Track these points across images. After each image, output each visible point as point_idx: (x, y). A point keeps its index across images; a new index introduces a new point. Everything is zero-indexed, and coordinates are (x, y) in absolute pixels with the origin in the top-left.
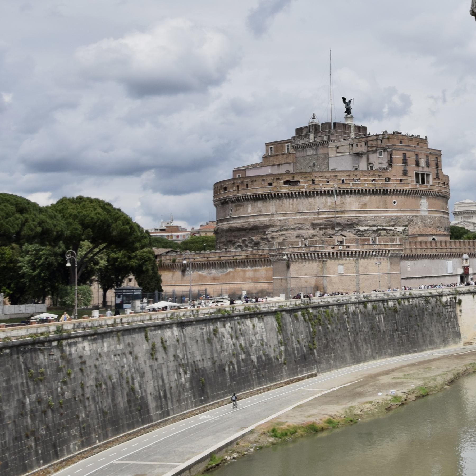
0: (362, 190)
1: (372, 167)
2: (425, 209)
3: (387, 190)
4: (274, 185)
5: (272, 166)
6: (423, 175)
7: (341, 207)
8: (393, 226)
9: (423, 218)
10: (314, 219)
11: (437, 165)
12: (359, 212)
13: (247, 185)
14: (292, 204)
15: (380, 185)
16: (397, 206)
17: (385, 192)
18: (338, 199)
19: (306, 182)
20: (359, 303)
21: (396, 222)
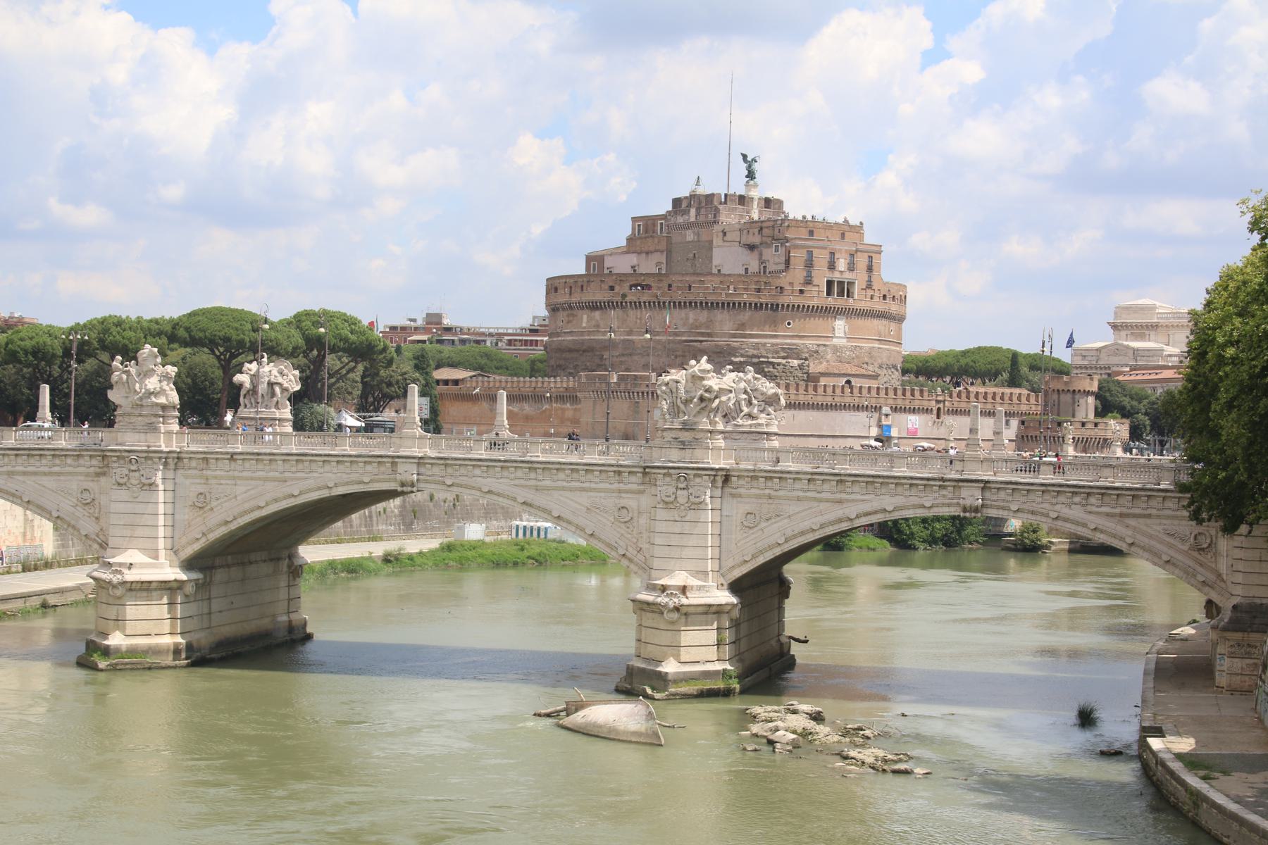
5: (639, 253)
6: (841, 283)
7: (708, 327)
8: (784, 358)
9: (836, 349)
10: (669, 342)
12: (734, 336)
18: (703, 316)
19: (659, 288)
21: (792, 353)
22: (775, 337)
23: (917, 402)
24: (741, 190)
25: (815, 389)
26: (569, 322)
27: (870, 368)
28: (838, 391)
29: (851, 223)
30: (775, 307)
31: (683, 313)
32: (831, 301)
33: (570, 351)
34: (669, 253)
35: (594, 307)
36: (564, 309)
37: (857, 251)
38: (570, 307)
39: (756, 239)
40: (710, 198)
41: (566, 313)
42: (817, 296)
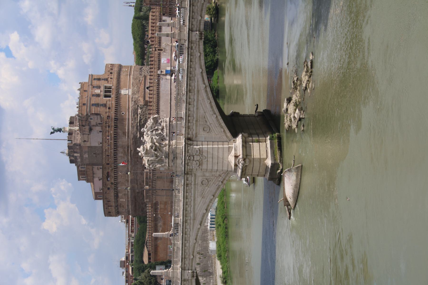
0: (115, 134)
1: (99, 124)
2: (128, 91)
3: (115, 118)
5: (93, 177)
6: (106, 92)
7: (125, 148)
8: (137, 116)
9: (133, 94)
10: (131, 164)
11: (99, 79)
12: (128, 136)
13: (108, 201)
14: (122, 176)
18: (120, 150)
19: (108, 168)
23: (156, 59)
24: (66, 134)
25: (150, 102)
26: (123, 207)
27: (141, 79)
28: (151, 92)
29: (80, 88)
30: (116, 119)
31: (119, 158)
33: (135, 206)
35: (117, 196)
36: (118, 209)
37: (92, 85)
38: (117, 206)
39: (87, 128)
40: (69, 147)
41: (119, 208)
42: (111, 101)
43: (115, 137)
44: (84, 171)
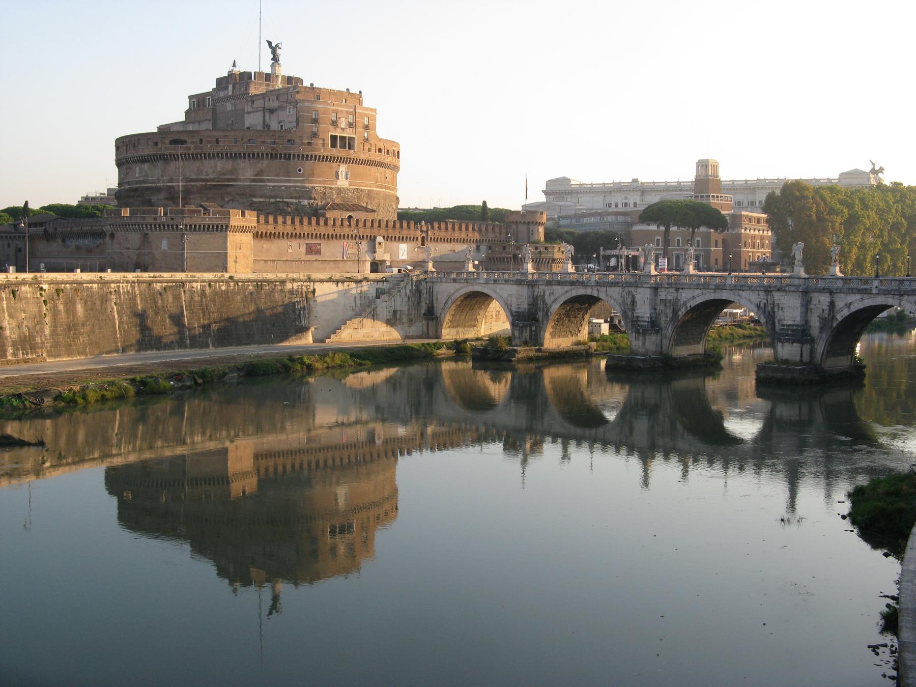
0: (258, 154)
3: (290, 155)
4: (160, 146)
7: (232, 174)
9: (339, 191)
12: (255, 181)
15: (281, 149)
16: (302, 175)
17: (288, 157)
18: (229, 165)
19: (193, 143)
20: (139, 282)
22: (289, 181)
24: (267, 69)
26: (127, 173)
28: (338, 223)
30: (288, 157)
31: (212, 162)
32: (337, 152)
34: (214, 121)
35: (143, 160)
39: (275, 104)
41: (125, 167)
43: (254, 154)
44: (204, 105)
